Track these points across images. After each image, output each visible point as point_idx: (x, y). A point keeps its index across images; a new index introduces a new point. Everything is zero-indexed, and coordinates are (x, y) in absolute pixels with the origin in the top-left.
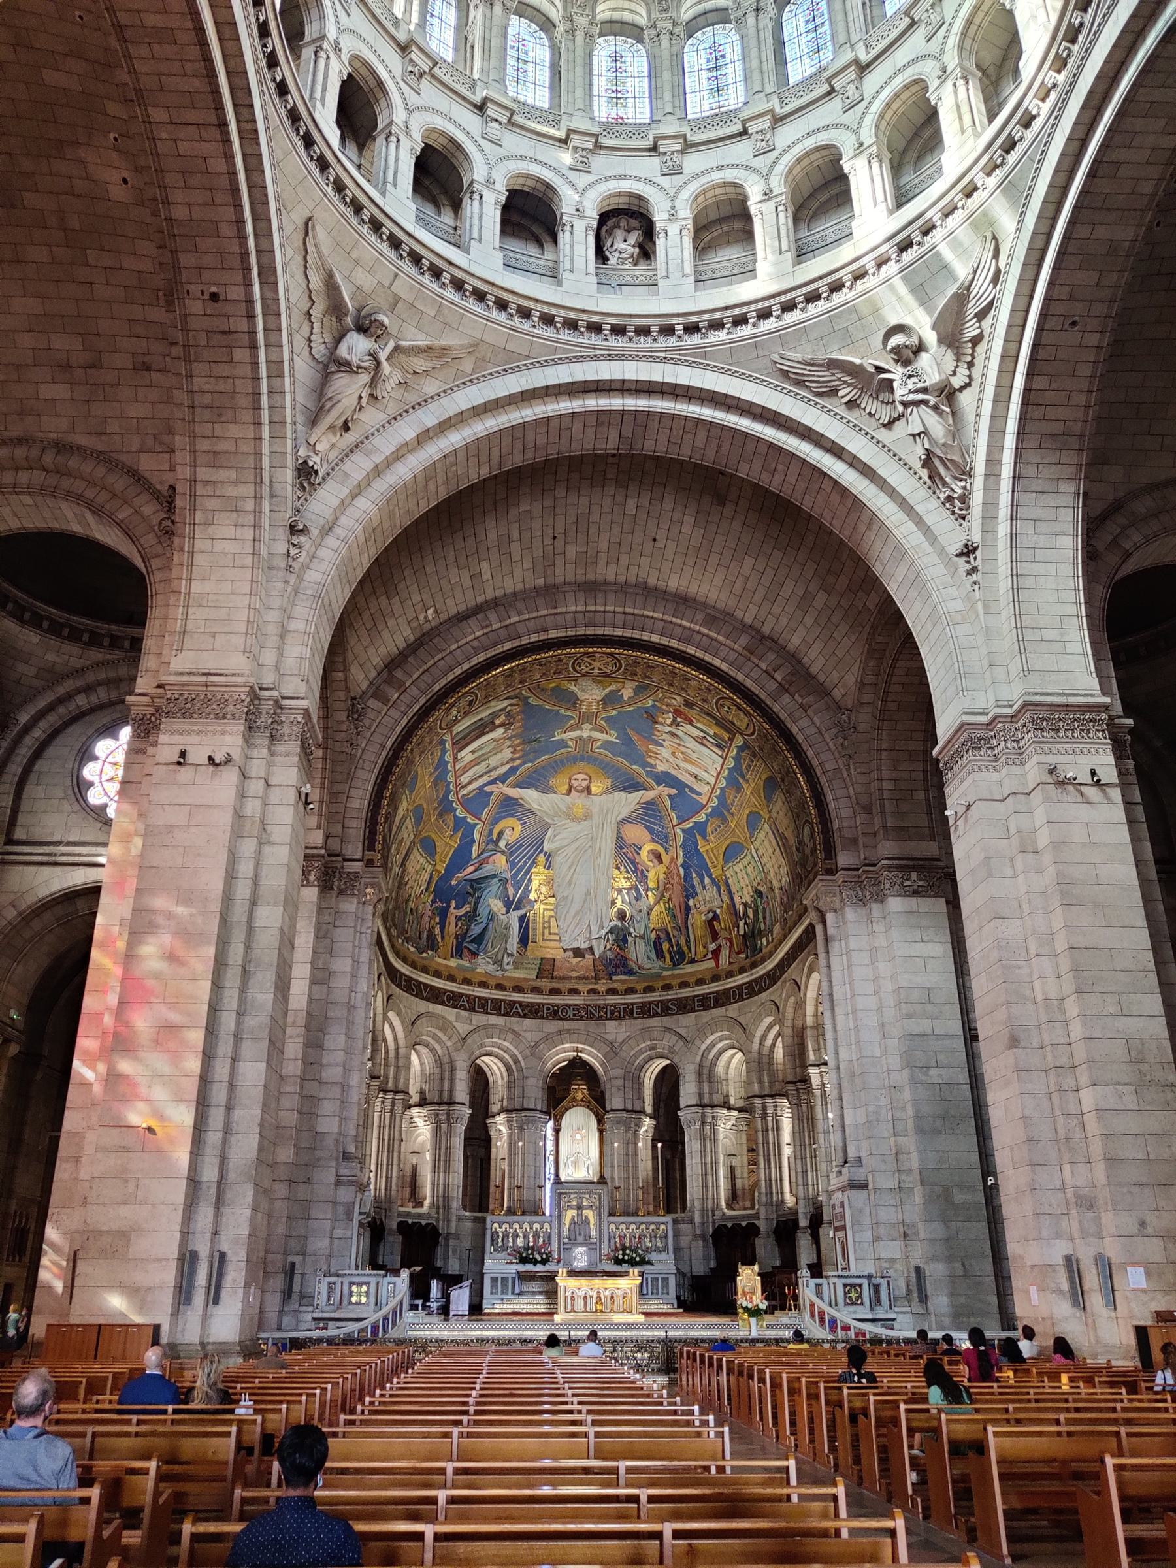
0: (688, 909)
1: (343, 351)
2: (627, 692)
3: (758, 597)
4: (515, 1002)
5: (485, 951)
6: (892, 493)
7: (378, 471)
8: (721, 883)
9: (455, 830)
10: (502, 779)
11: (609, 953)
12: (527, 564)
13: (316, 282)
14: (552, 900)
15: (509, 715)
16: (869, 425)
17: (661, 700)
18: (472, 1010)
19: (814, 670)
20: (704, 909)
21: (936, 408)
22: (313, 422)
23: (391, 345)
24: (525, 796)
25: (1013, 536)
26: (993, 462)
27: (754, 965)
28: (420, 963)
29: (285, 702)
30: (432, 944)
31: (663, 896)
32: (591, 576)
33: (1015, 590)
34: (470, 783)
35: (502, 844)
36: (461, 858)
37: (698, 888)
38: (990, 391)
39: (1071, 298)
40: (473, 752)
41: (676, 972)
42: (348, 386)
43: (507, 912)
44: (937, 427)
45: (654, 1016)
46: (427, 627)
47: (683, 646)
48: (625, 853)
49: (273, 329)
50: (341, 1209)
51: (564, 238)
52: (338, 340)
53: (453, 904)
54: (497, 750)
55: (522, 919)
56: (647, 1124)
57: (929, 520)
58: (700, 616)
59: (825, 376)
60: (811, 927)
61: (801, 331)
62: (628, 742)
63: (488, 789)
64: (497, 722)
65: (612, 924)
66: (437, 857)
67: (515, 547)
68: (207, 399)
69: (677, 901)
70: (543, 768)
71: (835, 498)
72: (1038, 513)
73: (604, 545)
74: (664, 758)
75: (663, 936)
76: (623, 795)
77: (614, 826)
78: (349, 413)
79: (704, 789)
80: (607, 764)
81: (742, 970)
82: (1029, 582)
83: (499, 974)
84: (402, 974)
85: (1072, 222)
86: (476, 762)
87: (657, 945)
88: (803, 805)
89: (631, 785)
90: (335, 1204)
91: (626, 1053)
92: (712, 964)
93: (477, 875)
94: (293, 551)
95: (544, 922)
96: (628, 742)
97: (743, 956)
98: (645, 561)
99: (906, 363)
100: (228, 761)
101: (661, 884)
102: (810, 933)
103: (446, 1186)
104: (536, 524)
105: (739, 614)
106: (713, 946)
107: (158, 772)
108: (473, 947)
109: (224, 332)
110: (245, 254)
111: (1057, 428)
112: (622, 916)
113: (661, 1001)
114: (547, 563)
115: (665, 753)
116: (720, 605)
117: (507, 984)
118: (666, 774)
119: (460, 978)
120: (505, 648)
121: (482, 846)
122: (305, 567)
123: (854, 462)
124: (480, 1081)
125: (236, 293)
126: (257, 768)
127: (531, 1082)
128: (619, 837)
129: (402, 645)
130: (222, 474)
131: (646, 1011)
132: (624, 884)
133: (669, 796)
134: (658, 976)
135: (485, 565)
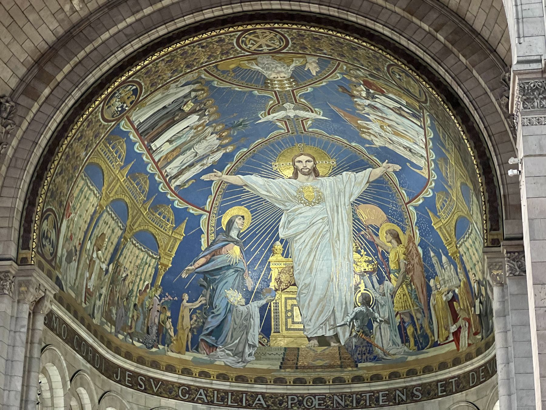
0: (429, 290)
2: (313, 68)
4: (257, 394)
5: (224, 343)
8: (457, 261)
9: (178, 222)
10: (219, 166)
11: (354, 340)
14: (292, 288)
17: (347, 72)
18: (211, 403)
19: (478, 26)
20: (444, 289)
24: (249, 183)
28: (148, 358)
31: (405, 277)
34: (181, 173)
35: (234, 234)
37: (437, 267)
40: (170, 141)
41: (421, 356)
43: (247, 303)
45: (399, 404)
46: (75, 18)
47: (343, 15)
53: (186, 297)
55: (263, 309)
62: (336, 118)
63: (205, 178)
64: (186, 109)
65: (357, 309)
66: (161, 251)
69: (418, 282)
70: (261, 152)
75: (407, 319)
76: (351, 174)
77: (349, 207)
80: (327, 143)
81: (479, 352)
83: (240, 365)
84: (124, 370)
87: (402, 329)
92: (453, 346)
93: (209, 267)
95: (287, 311)
97: (479, 337)
101: (402, 265)
106: (453, 328)
108: (211, 340)
113: (406, 387)
115: (375, 127)
117: (248, 375)
118: (384, 149)
119: (196, 370)
120: (161, 33)
121: (212, 237)
128: (356, 219)
129: (51, 39)
132: (364, 266)
133: (395, 172)
134: (402, 362)
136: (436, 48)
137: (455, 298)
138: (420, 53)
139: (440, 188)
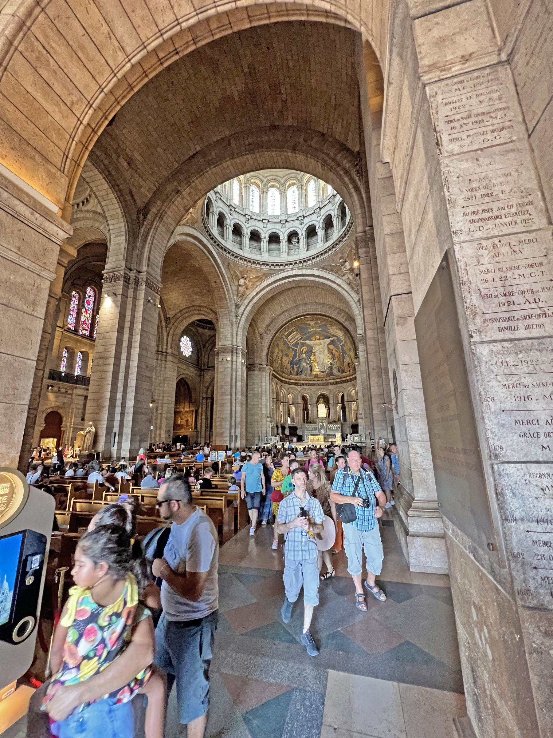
7: (250, 302)
13: (232, 273)
30: (291, 374)
48: (330, 351)
49: (226, 284)
56: (339, 406)
61: (325, 260)
89: (328, 338)
114: (295, 301)
123: (338, 285)
126: (234, 360)
128: (328, 348)
131: (337, 383)
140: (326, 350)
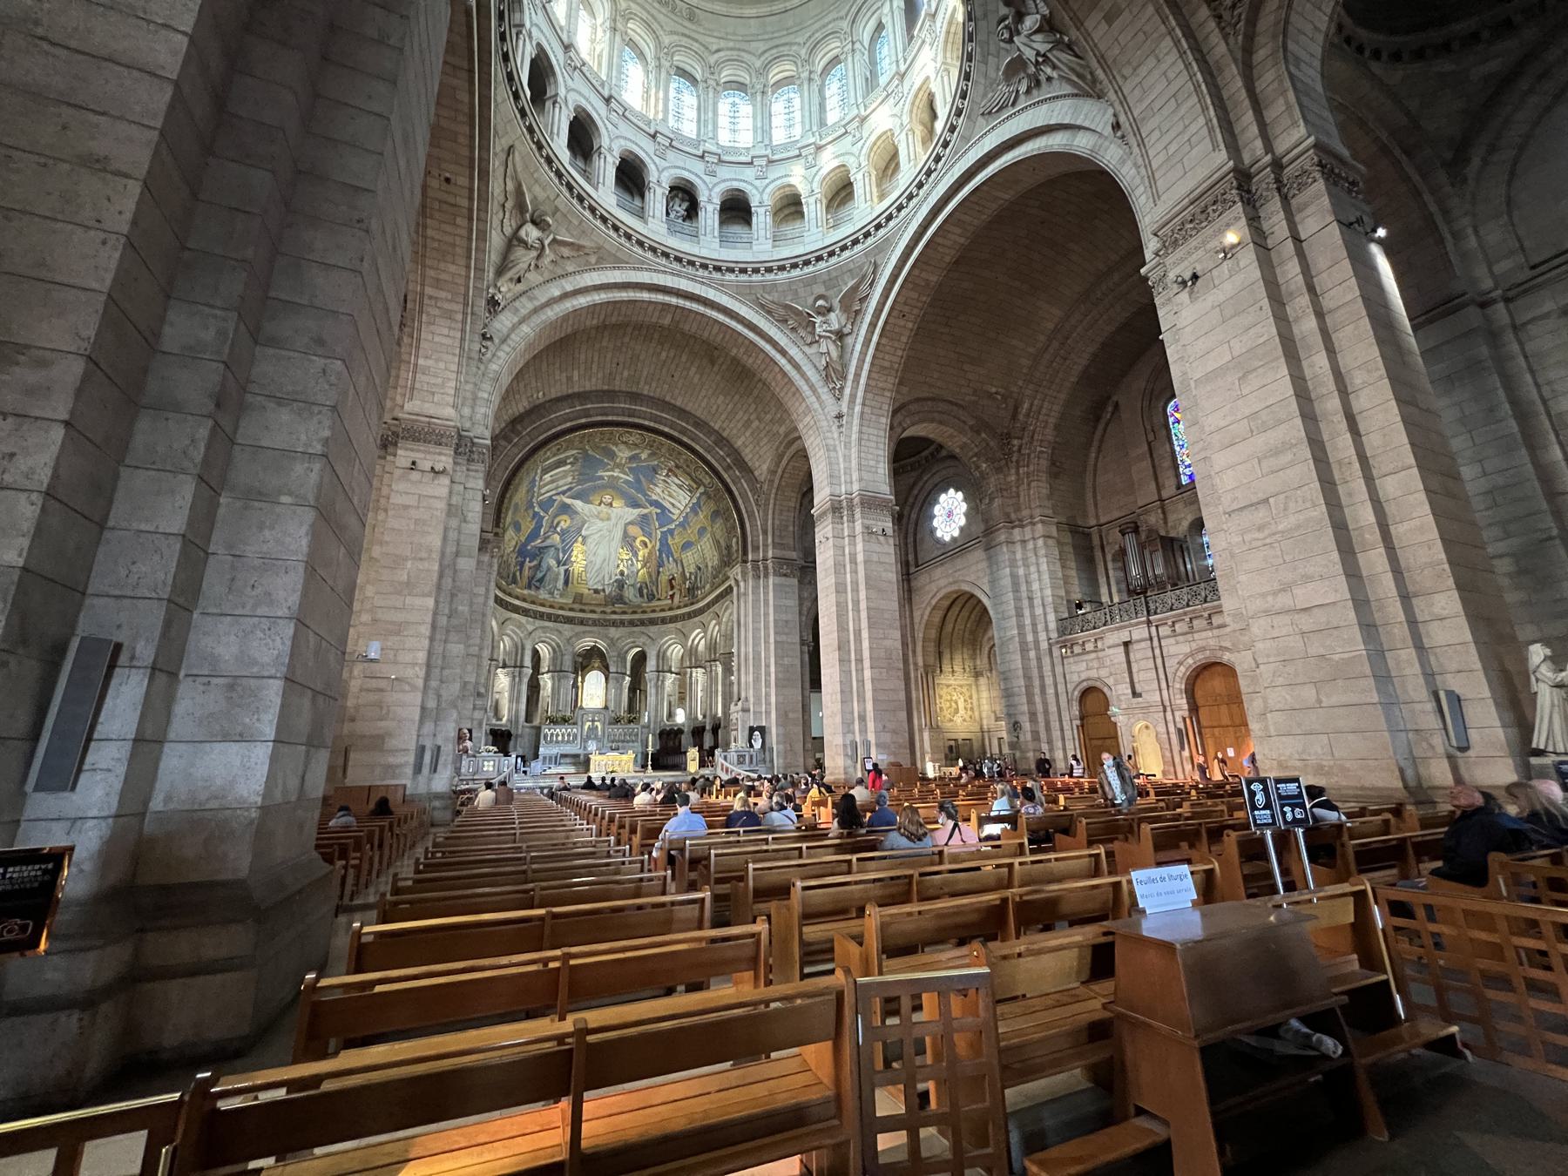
1: (522, 233)
2: (643, 456)
3: (723, 417)
6: (807, 380)
7: (536, 311)
10: (564, 493)
12: (600, 375)
13: (510, 186)
15: (576, 459)
16: (800, 343)
19: (746, 460)
21: (834, 342)
22: (500, 271)
23: (551, 237)
25: (862, 413)
26: (857, 376)
27: (692, 604)
29: (476, 440)
30: (514, 581)
32: (634, 390)
33: (860, 440)
36: (534, 535)
38: (861, 339)
39: (905, 304)
42: (525, 255)
44: (834, 354)
46: (538, 402)
47: (680, 436)
48: (628, 541)
49: (483, 209)
50: (475, 723)
51: (649, 196)
52: (520, 227)
54: (564, 477)
55: (567, 571)
56: (628, 679)
57: (824, 397)
58: (691, 421)
59: (782, 312)
60: (730, 588)
61: (774, 286)
62: (638, 481)
67: (595, 366)
68: (436, 245)
69: (653, 570)
71: (779, 377)
72: (874, 403)
73: (645, 373)
74: (657, 492)
76: (631, 510)
78: (522, 273)
79: (678, 512)
81: (686, 606)
82: (866, 437)
85: (914, 266)
86: (552, 482)
88: (734, 527)
89: (635, 504)
90: (472, 720)
91: (620, 644)
94: (483, 350)
96: (638, 481)
98: (666, 386)
99: (823, 315)
100: (444, 472)
102: (729, 590)
103: (517, 711)
104: (609, 355)
105: (712, 424)
107: (398, 472)
109: (452, 205)
110: (472, 159)
111: (887, 364)
112: (622, 573)
116: (703, 417)
118: (656, 501)
122: (490, 361)
123: (791, 361)
124: (536, 655)
125: (462, 181)
127: (566, 657)
128: (625, 532)
129: (522, 410)
130: (443, 294)
131: (632, 623)
135: (576, 373)
136: (725, 464)
137: (673, 578)
138: (716, 465)
139: (681, 525)
140: (619, 534)
